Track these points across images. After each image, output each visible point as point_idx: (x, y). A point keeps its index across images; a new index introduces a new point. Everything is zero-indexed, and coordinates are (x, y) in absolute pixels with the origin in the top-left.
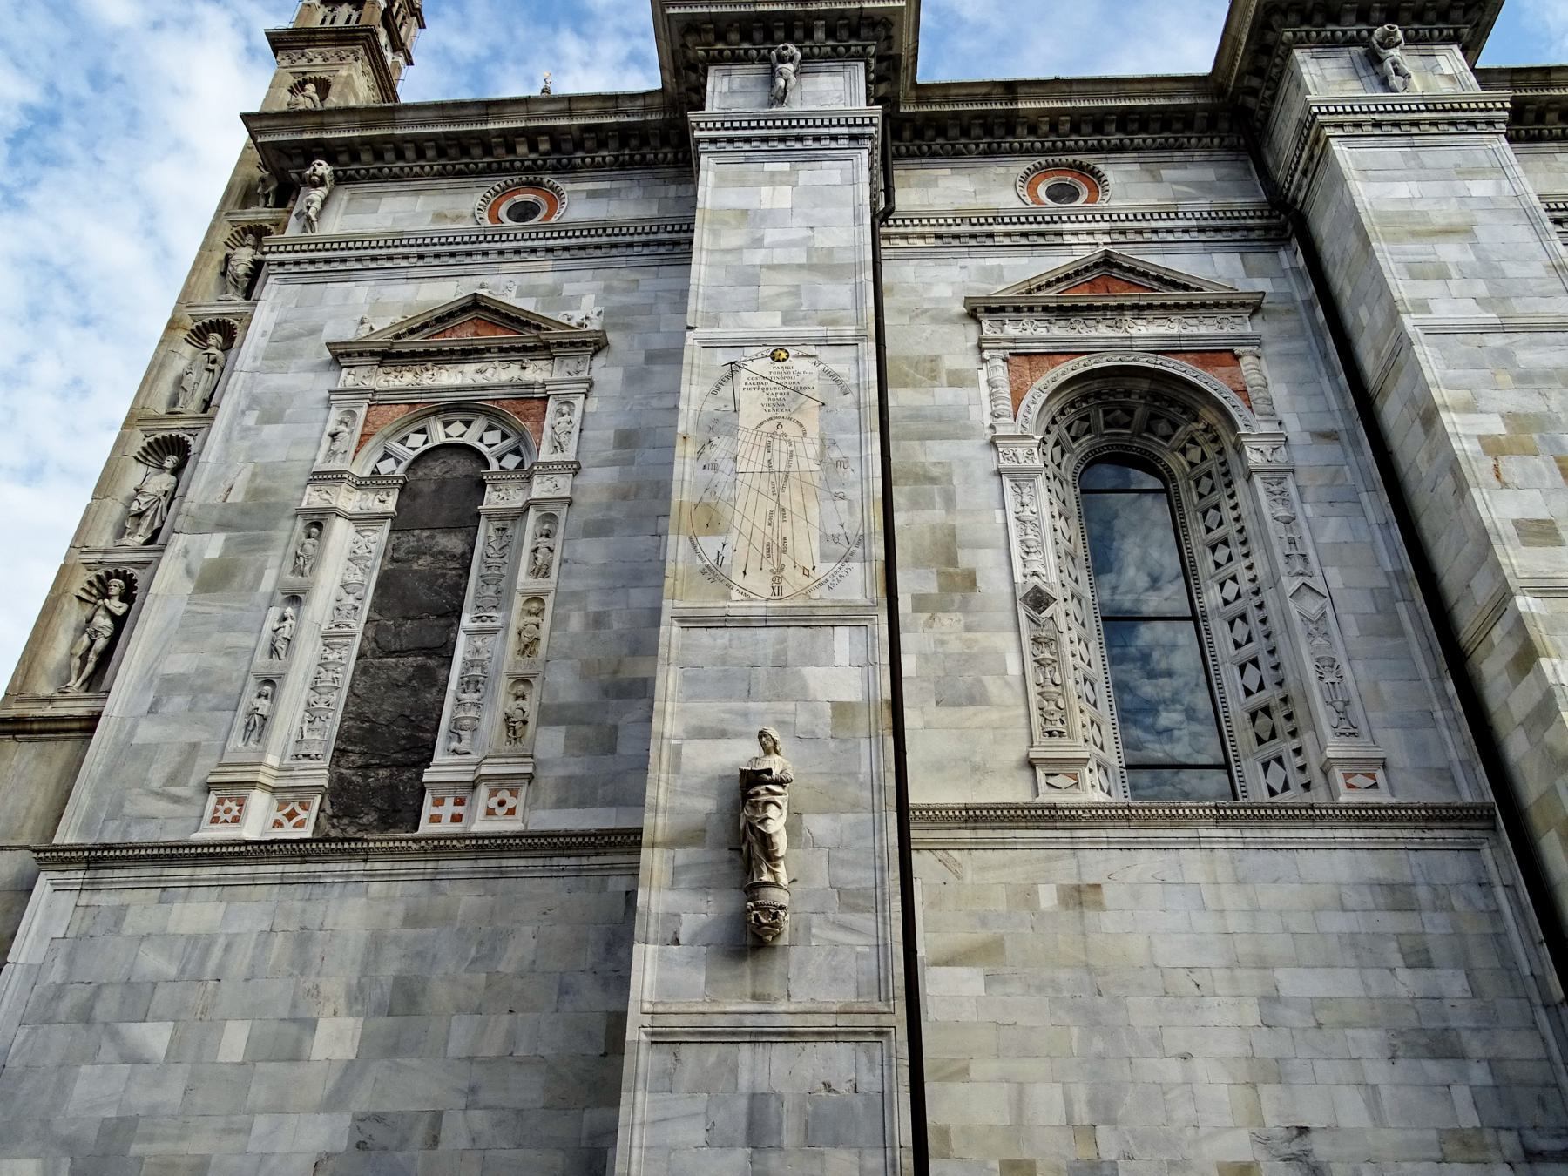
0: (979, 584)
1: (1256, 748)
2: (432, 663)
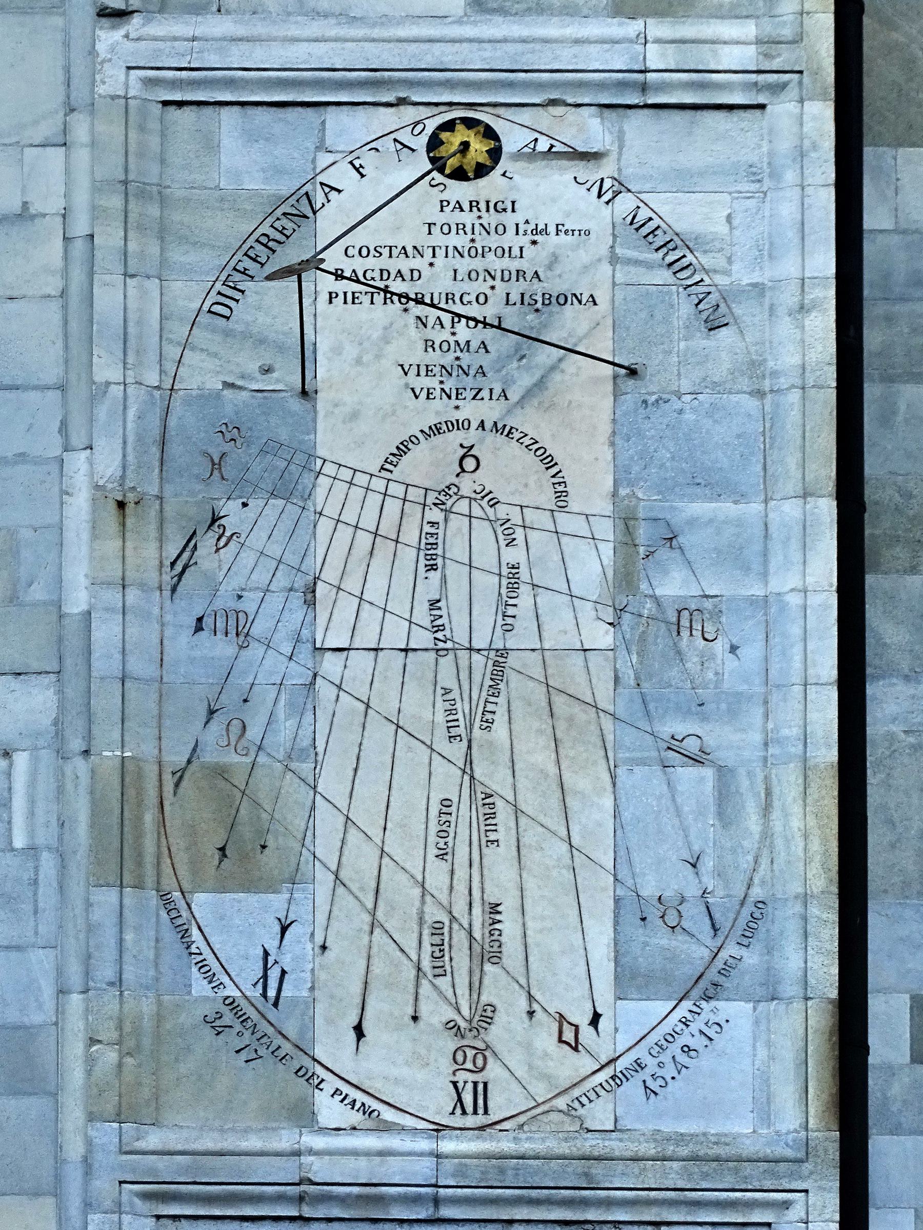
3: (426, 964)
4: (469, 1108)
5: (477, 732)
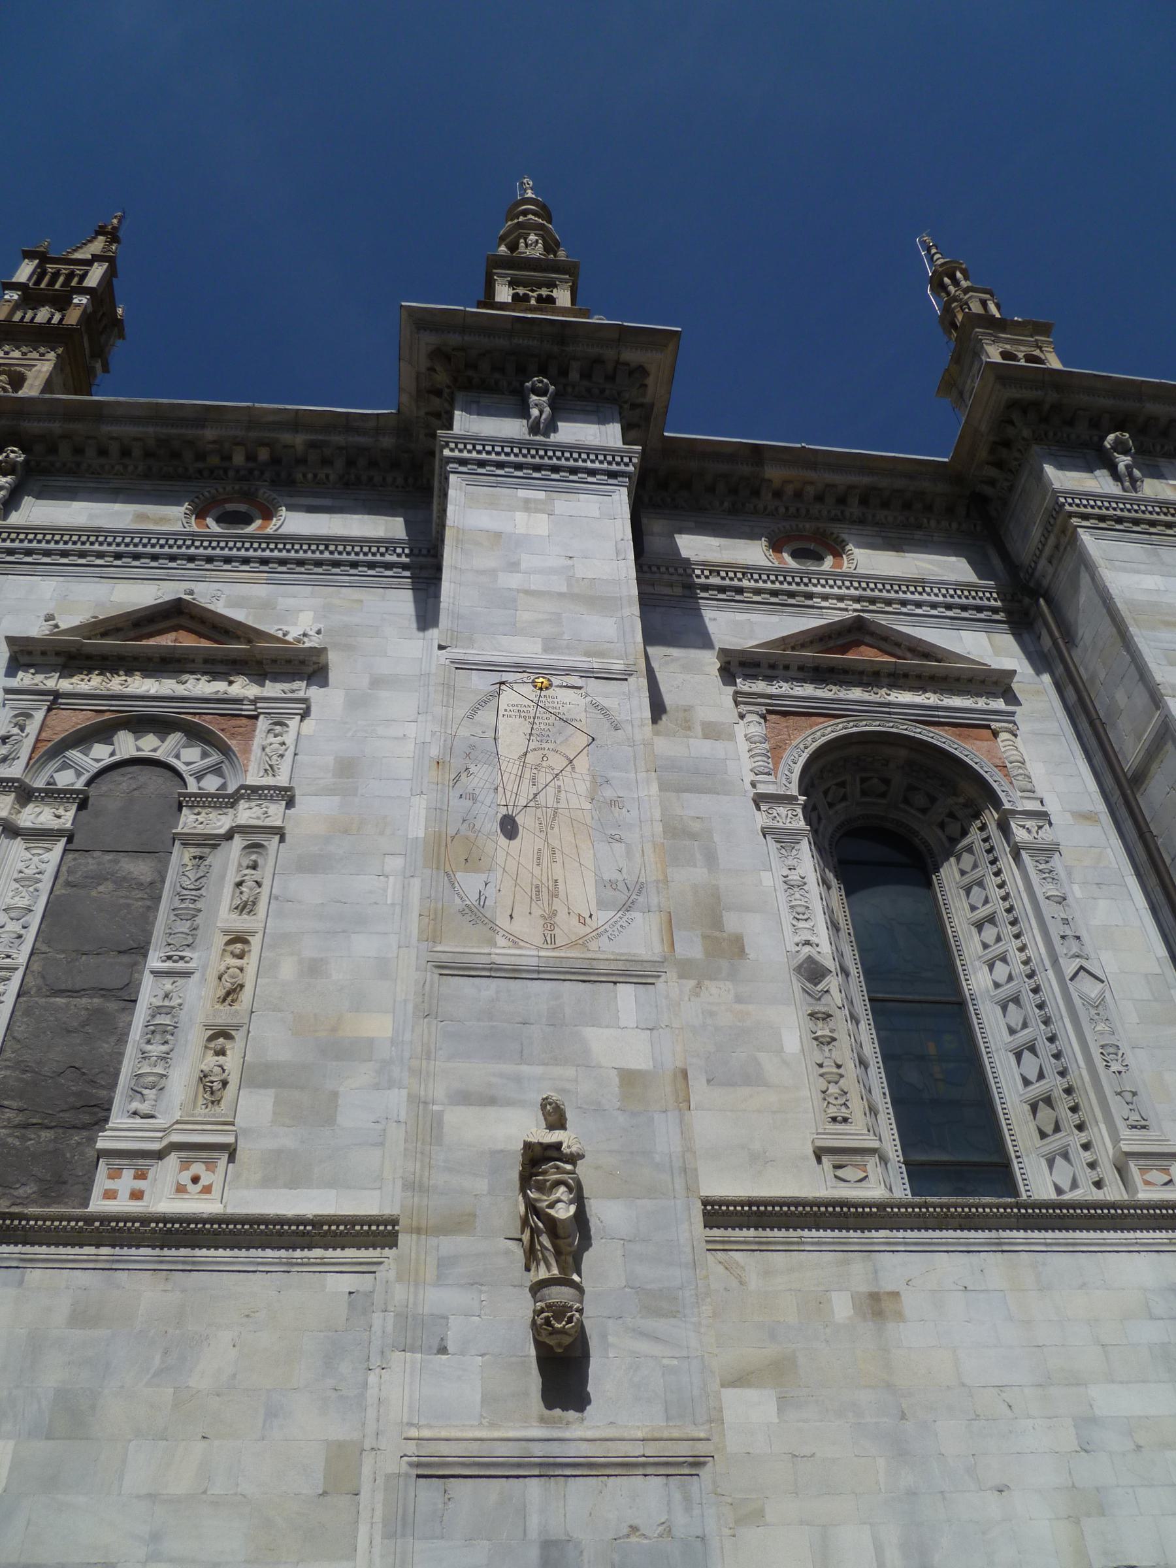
0: (747, 951)
1: (1038, 1142)
2: (112, 1006)
3: (534, 897)
4: (549, 942)
5: (549, 830)
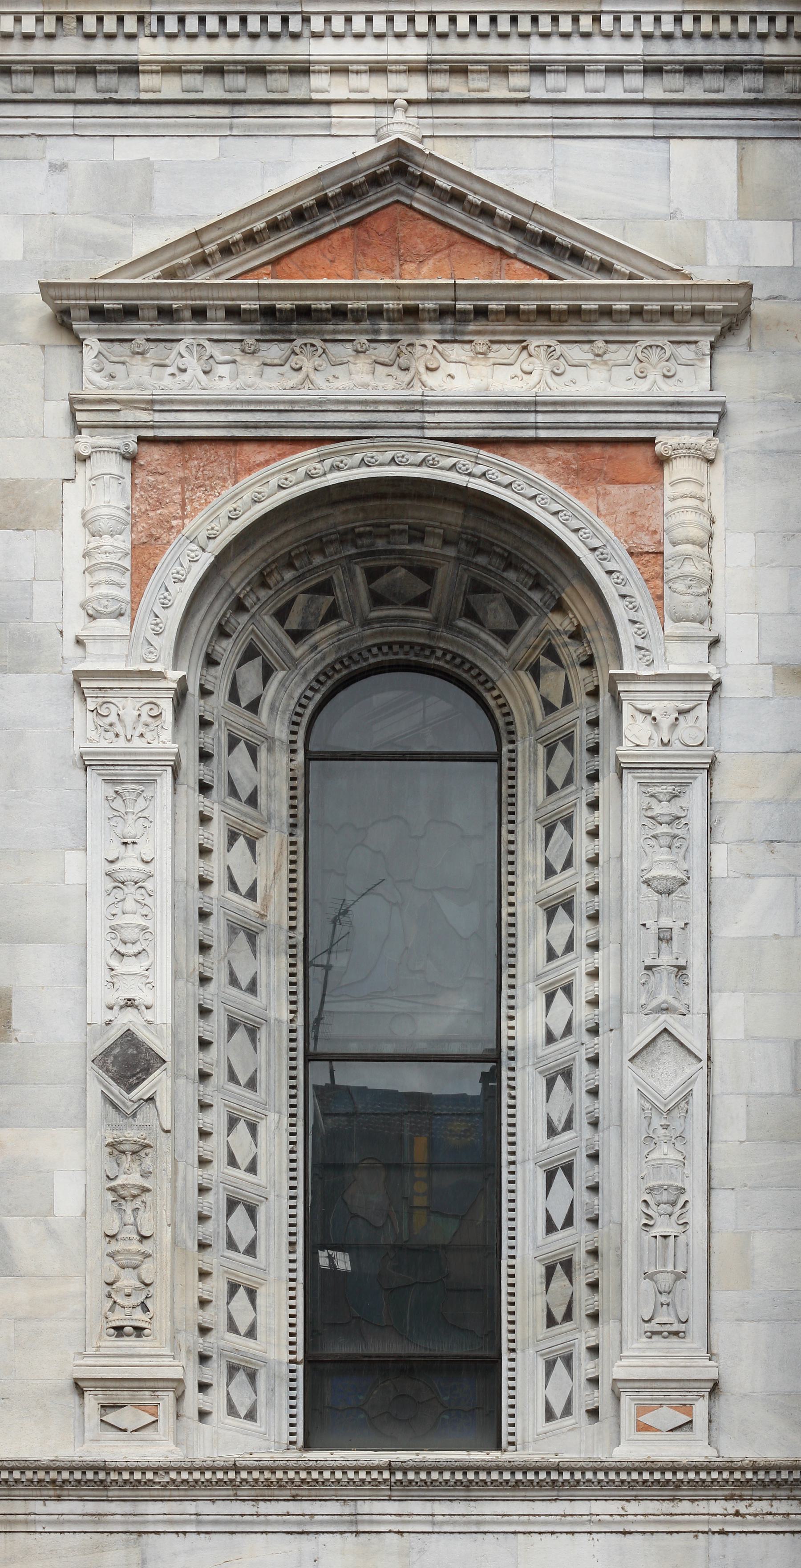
0: (15, 1025)
